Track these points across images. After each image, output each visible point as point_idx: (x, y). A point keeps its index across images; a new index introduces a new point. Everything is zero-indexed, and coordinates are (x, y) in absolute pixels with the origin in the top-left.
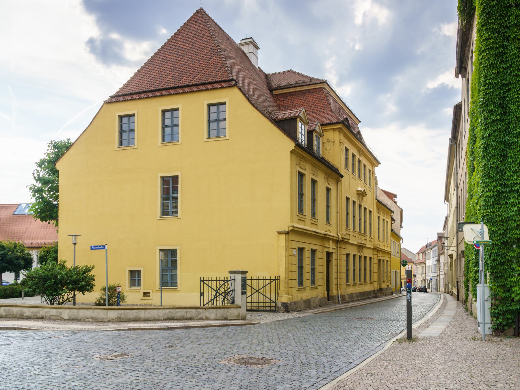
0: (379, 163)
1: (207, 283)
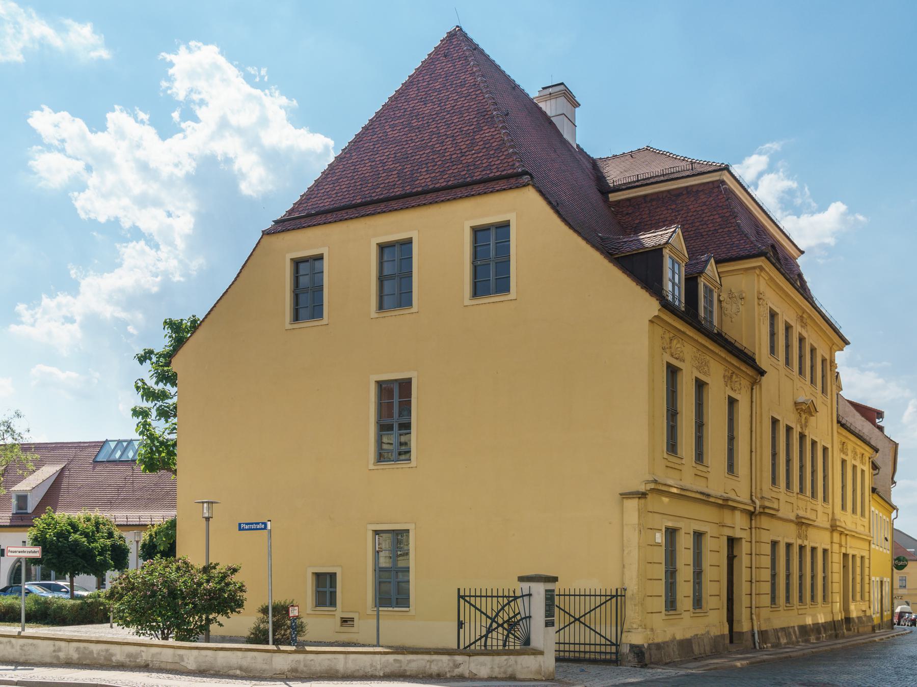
1: (472, 600)
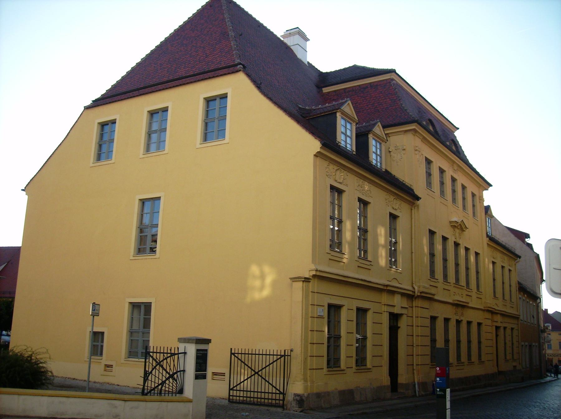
0: (491, 185)
1: (240, 356)
